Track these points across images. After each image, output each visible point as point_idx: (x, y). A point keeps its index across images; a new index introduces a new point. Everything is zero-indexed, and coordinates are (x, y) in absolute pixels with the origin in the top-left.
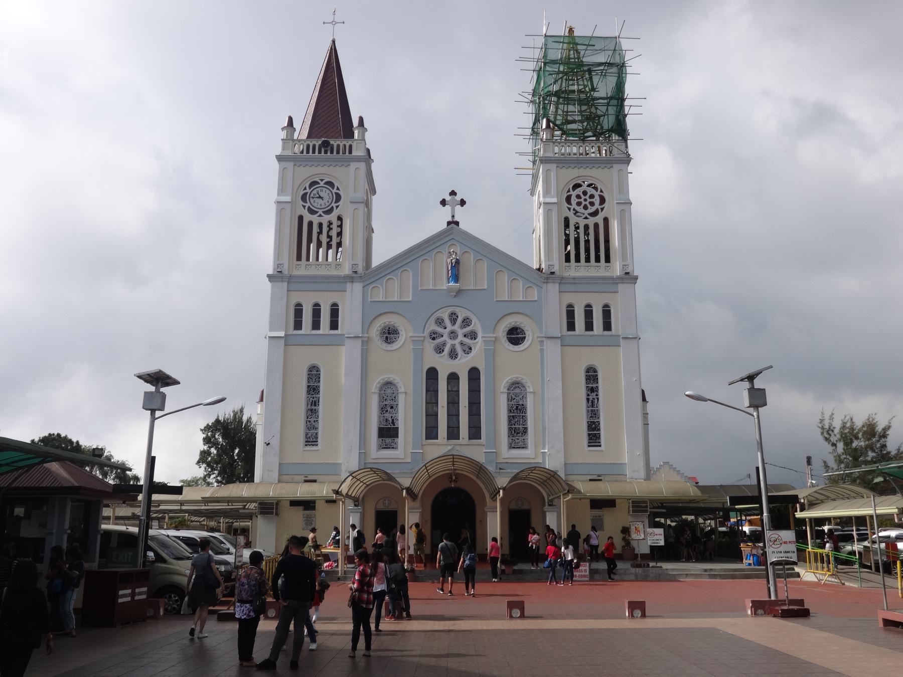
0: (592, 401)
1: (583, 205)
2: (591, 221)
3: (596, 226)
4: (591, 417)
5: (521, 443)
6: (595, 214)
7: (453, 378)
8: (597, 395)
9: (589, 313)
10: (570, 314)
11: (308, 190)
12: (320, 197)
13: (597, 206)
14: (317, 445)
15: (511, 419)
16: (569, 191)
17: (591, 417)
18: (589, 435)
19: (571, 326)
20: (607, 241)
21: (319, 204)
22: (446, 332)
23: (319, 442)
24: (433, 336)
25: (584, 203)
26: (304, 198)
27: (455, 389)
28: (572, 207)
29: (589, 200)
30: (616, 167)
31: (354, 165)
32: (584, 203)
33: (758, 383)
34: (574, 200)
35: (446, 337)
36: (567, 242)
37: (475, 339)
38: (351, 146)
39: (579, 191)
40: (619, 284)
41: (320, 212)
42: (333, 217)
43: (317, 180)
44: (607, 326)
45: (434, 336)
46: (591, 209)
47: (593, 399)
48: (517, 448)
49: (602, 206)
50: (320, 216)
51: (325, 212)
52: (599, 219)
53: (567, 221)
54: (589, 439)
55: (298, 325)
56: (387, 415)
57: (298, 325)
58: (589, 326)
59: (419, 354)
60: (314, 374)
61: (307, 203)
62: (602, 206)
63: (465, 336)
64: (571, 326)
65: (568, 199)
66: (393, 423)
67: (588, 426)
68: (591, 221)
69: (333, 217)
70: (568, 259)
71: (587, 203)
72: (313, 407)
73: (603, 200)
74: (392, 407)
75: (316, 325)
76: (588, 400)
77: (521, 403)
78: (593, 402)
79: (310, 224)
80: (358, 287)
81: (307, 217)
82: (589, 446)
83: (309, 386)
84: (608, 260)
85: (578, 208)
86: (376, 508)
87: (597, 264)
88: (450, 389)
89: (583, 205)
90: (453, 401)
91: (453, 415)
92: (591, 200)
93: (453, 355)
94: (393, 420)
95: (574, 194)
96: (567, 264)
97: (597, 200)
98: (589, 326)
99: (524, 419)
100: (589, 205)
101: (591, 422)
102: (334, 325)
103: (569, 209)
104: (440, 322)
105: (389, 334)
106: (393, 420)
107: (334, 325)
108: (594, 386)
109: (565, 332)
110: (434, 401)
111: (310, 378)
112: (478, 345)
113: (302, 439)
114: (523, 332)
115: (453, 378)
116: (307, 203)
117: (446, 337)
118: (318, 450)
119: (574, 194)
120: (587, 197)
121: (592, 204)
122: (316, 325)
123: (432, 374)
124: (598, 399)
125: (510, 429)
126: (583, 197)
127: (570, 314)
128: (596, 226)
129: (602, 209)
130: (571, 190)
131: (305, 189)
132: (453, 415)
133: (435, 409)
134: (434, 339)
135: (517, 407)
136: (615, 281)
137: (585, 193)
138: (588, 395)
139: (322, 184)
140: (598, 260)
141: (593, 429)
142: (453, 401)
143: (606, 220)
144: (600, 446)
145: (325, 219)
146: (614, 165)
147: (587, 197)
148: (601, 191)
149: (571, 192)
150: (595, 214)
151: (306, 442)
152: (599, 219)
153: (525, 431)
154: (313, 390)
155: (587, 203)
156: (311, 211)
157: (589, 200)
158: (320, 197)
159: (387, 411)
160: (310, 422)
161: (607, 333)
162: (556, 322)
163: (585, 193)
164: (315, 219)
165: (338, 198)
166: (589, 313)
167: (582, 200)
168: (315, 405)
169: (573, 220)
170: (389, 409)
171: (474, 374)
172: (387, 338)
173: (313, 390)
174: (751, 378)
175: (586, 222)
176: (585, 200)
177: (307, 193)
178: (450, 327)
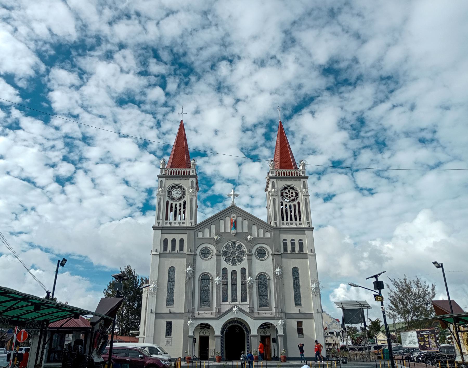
1: (288, 196)
2: (292, 204)
3: (295, 205)
6: (294, 200)
12: (177, 193)
16: (282, 190)
20: (299, 212)
21: (177, 196)
25: (289, 196)
29: (291, 194)
30: (302, 181)
31: (191, 180)
32: (289, 196)
33: (380, 279)
36: (282, 212)
38: (189, 171)
40: (306, 231)
41: (176, 199)
44: (301, 249)
46: (292, 198)
49: (297, 197)
50: (176, 201)
55: (165, 249)
57: (165, 249)
58: (293, 249)
59: (218, 261)
61: (170, 195)
62: (297, 197)
65: (282, 194)
69: (182, 202)
70: (283, 220)
73: (297, 194)
79: (172, 204)
81: (170, 202)
84: (300, 219)
86: (199, 335)
89: (288, 196)
90: (234, 284)
91: (234, 290)
92: (292, 194)
96: (283, 222)
97: (294, 194)
100: (291, 197)
108: (297, 276)
110: (226, 284)
112: (245, 258)
115: (234, 272)
116: (170, 195)
120: (290, 193)
121: (292, 196)
128: (295, 205)
129: (297, 198)
130: (283, 190)
131: (170, 189)
132: (234, 290)
133: (226, 287)
135: (263, 286)
136: (304, 229)
138: (295, 281)
142: (234, 284)
143: (299, 203)
146: (301, 180)
147: (290, 193)
148: (296, 190)
152: (296, 203)
155: (290, 195)
156: (172, 199)
157: (291, 194)
158: (177, 193)
163: (289, 191)
164: (174, 203)
174: (376, 277)
176: (289, 194)
177: (170, 191)
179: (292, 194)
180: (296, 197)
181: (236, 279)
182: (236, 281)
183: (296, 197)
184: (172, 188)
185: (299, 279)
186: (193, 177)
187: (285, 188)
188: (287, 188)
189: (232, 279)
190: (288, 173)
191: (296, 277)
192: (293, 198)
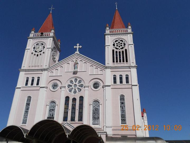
0: (122, 107)
3: (123, 52)
4: (122, 113)
5: (97, 123)
6: (123, 48)
7: (74, 100)
8: (124, 105)
9: (121, 78)
10: (115, 79)
11: (36, 46)
13: (123, 46)
14: (26, 124)
15: (94, 113)
16: (114, 42)
17: (122, 113)
18: (121, 119)
19: (115, 82)
22: (73, 85)
23: (27, 123)
24: (69, 86)
25: (119, 45)
26: (34, 48)
27: (74, 104)
28: (115, 47)
31: (49, 39)
32: (120, 45)
34: (116, 45)
35: (73, 87)
37: (82, 87)
38: (49, 34)
39: (117, 42)
42: (42, 53)
43: (39, 43)
44: (127, 82)
45: (69, 86)
46: (121, 47)
47: (123, 106)
48: (95, 124)
51: (40, 52)
52: (124, 50)
53: (113, 51)
54: (122, 121)
55: (27, 84)
56: (51, 112)
58: (121, 82)
60: (29, 98)
63: (79, 86)
64: (115, 82)
65: (114, 45)
66: (53, 115)
67: (121, 116)
68: (121, 50)
70: (114, 62)
71: (120, 45)
72: (27, 110)
73: (125, 44)
74: (53, 110)
75: (32, 84)
76: (121, 107)
77: (97, 108)
78: (122, 107)
80: (46, 72)
82: (122, 124)
83: (27, 103)
84: (127, 61)
85: (117, 47)
87: (123, 63)
88: (73, 104)
89: (118, 46)
90: (74, 108)
93: (75, 92)
94: (53, 115)
95: (116, 43)
96: (114, 63)
97: (123, 45)
98: (121, 82)
99: (99, 114)
101: (122, 115)
102: (38, 84)
103: (114, 47)
104: (71, 82)
105: (55, 86)
106: (53, 115)
107: (38, 84)
108: (123, 102)
109: (113, 84)
110: (67, 108)
111: (27, 101)
113: (22, 122)
114: (98, 84)
115: (74, 100)
117: (73, 87)
118: (25, 126)
119: (116, 43)
120: (120, 44)
122: (32, 84)
123: (67, 98)
124: (124, 106)
125: (93, 117)
126: (118, 44)
127: (115, 79)
128: (123, 52)
129: (125, 47)
133: (67, 110)
134: (69, 87)
135: (96, 110)
137: (119, 43)
138: (121, 105)
139: (40, 44)
140: (123, 61)
141: (123, 117)
142: (74, 108)
143: (126, 50)
144: (126, 124)
145: (40, 53)
149: (115, 43)
150: (123, 48)
151: (23, 122)
153: (98, 118)
154: (28, 104)
156: (36, 52)
159: (51, 111)
160: (25, 115)
161: (127, 84)
162: (109, 80)
164: (36, 53)
165: (44, 47)
166: (121, 78)
167: (118, 45)
168: (28, 110)
169: (115, 50)
170: (52, 111)
171: (82, 98)
172: (54, 88)
173: (28, 104)
175: (119, 51)
176: (119, 45)
178: (74, 83)
179: (121, 44)
180: (124, 46)
181: (75, 104)
182: (75, 106)
183: (124, 46)
184: (37, 45)
185: (124, 104)
186: (51, 37)
187: (116, 41)
188: (118, 41)
189: (72, 104)
190: (119, 32)
191: (122, 103)
192: (122, 47)
